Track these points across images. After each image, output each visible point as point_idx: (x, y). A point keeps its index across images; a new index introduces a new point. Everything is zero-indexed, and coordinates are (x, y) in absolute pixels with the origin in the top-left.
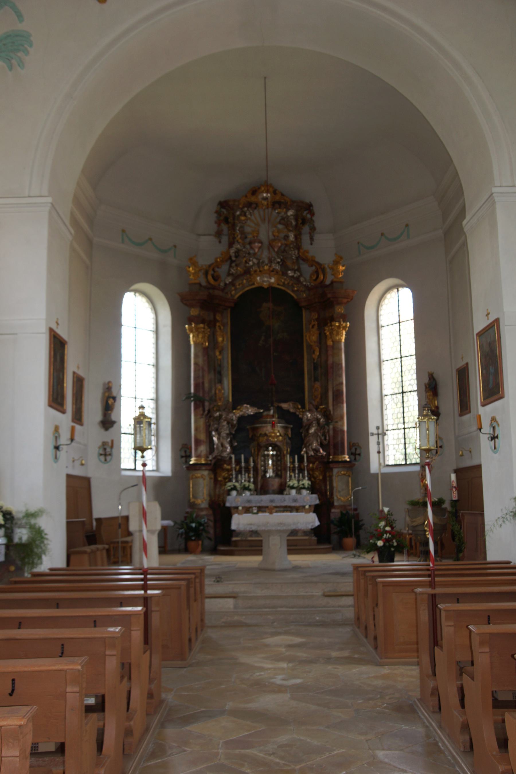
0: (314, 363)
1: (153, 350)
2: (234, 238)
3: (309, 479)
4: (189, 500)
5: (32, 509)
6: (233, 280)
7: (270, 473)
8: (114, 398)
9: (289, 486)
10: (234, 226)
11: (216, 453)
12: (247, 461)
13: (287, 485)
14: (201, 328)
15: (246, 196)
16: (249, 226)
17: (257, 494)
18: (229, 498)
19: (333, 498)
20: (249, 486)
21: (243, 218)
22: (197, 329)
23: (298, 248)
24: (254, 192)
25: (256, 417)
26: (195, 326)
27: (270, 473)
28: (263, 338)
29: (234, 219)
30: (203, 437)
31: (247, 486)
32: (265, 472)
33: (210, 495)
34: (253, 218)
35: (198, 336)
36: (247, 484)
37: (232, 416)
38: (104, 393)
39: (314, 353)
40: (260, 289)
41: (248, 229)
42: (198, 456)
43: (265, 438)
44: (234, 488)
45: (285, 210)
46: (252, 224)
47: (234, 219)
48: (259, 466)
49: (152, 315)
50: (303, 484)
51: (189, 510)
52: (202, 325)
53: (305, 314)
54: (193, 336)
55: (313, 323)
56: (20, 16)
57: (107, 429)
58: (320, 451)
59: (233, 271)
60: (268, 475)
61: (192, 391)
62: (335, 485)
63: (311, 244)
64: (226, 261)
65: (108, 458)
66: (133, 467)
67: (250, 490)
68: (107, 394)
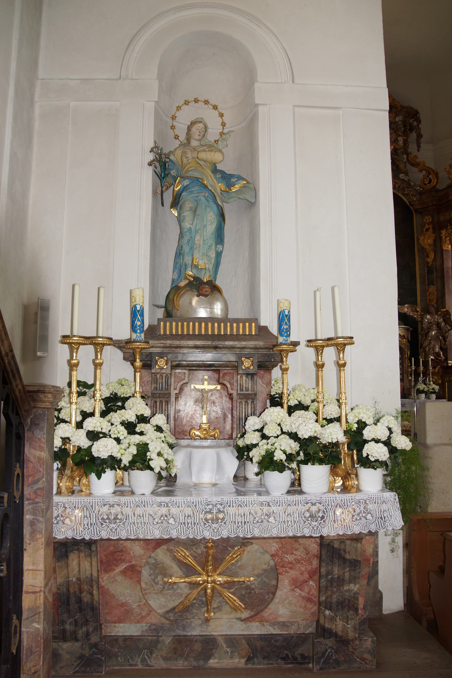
0: (428, 267)
23: (408, 154)
39: (428, 257)
53: (416, 219)
55: (427, 227)
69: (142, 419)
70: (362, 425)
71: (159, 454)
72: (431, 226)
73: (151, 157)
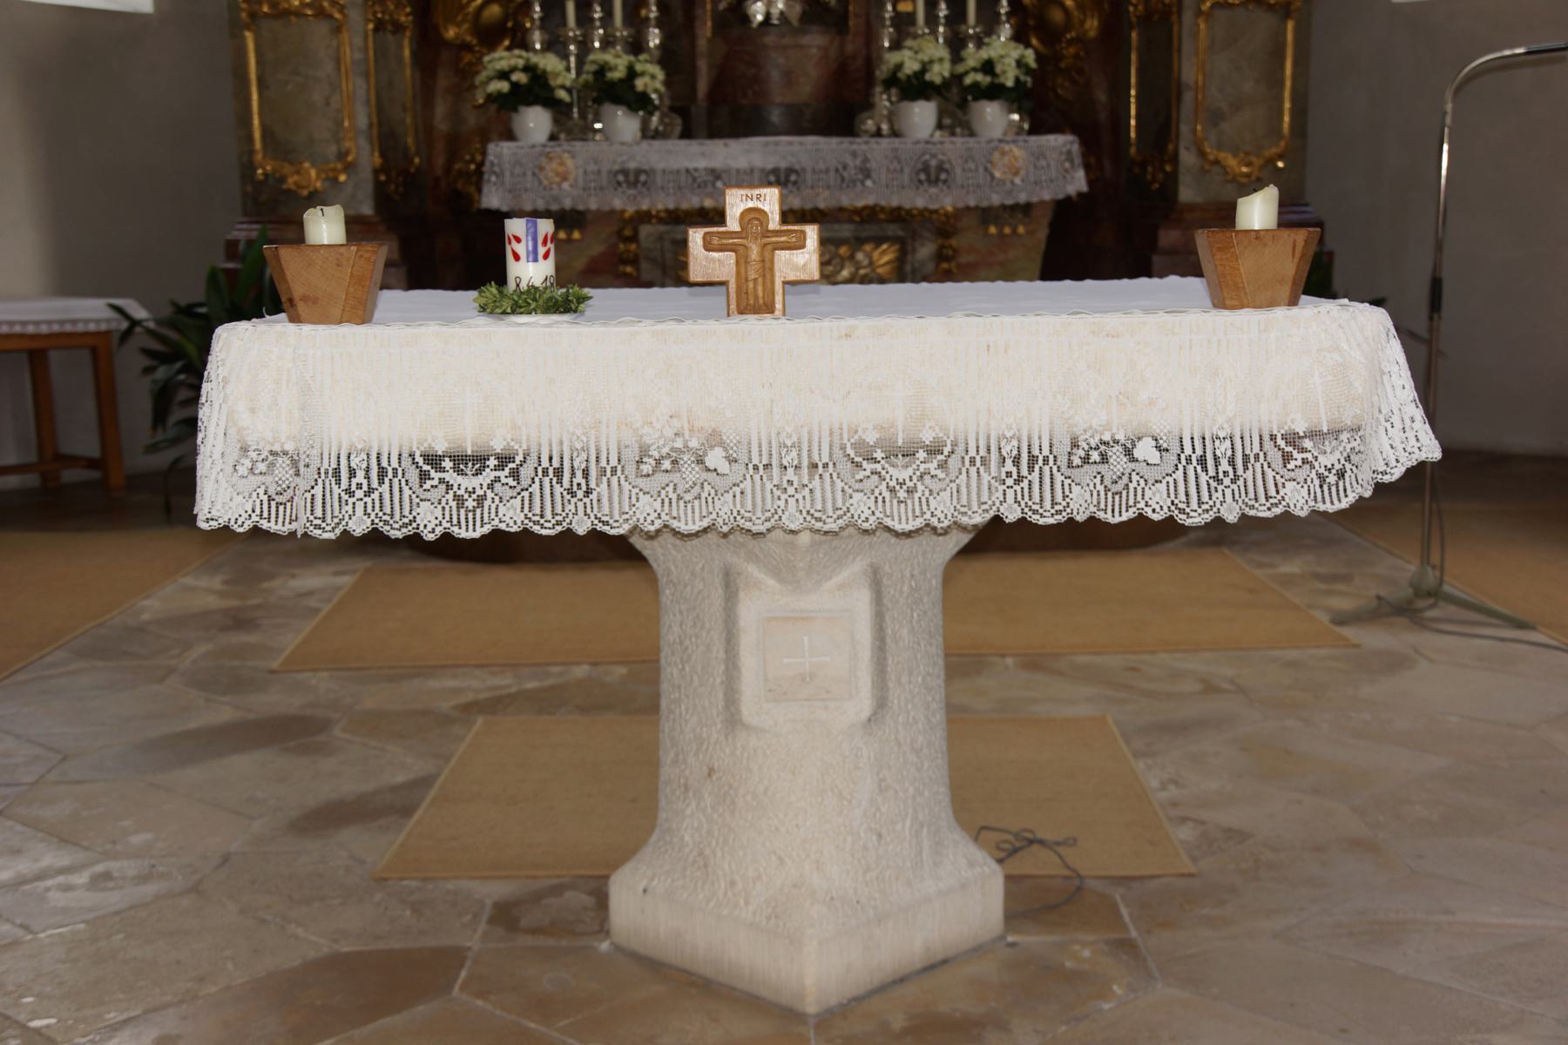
3: (1019, 37)
4: (248, 168)
9: (892, 81)
13: (882, 72)
17: (687, 134)
18: (500, 151)
19: (1175, 159)
20: (632, 74)
33: (386, 138)
36: (618, 62)
44: (536, 90)
50: (988, 67)
51: (243, 232)
62: (1189, 71)
67: (639, 103)
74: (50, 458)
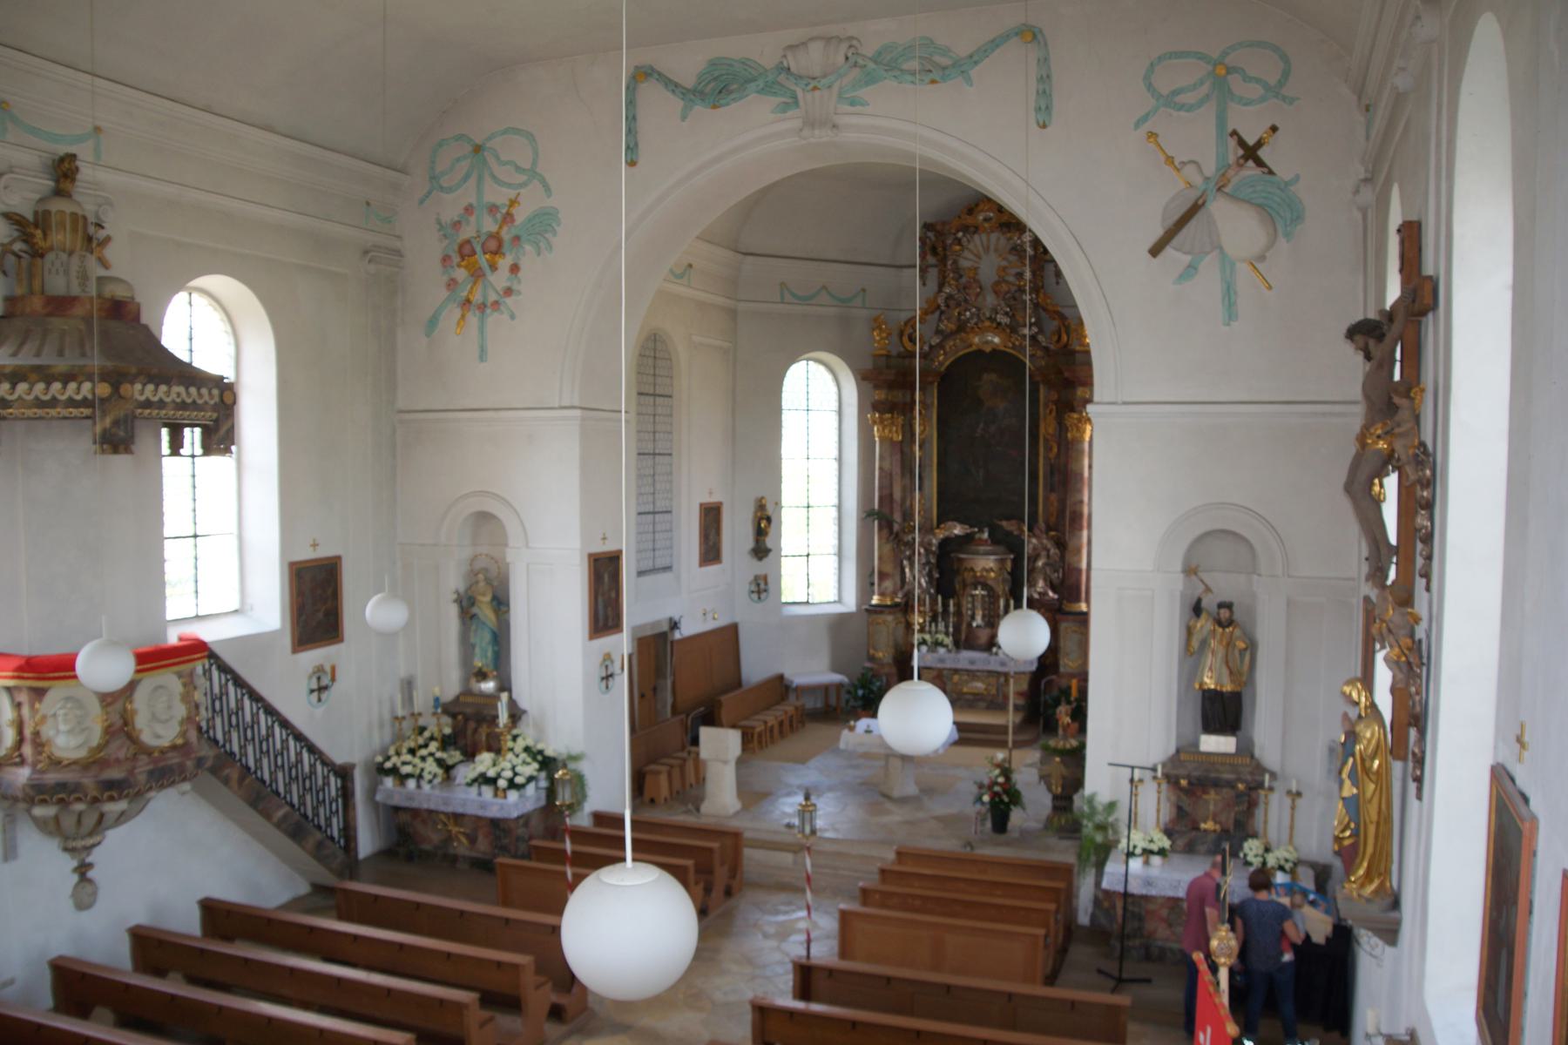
1: (836, 438)
2: (944, 277)
4: (868, 652)
5: (575, 751)
6: (942, 341)
7: (978, 621)
8: (769, 520)
10: (943, 261)
11: (906, 588)
12: (945, 606)
14: (887, 419)
15: (959, 217)
16: (966, 258)
21: (958, 248)
22: (882, 421)
24: (971, 211)
25: (966, 541)
26: (879, 417)
27: (978, 621)
28: (981, 425)
29: (945, 249)
30: (888, 568)
31: (940, 640)
32: (973, 617)
34: (971, 246)
35: (883, 429)
36: (940, 637)
37: (931, 540)
38: (756, 513)
40: (980, 352)
41: (964, 264)
42: (882, 594)
43: (971, 574)
45: (1017, 234)
46: (971, 256)
47: (945, 249)
48: (964, 611)
49: (834, 389)
51: (868, 665)
52: (888, 416)
54: (878, 429)
56: (547, 189)
57: (760, 559)
58: (1047, 594)
59: (942, 326)
60: (974, 624)
61: (876, 507)
63: (1058, 283)
64: (933, 312)
65: (763, 595)
66: (806, 600)
67: (946, 646)
68: (759, 514)
69: (432, 754)
70: (503, 770)
71: (430, 773)
72: (1054, 407)
73: (455, 596)
74: (827, 705)
